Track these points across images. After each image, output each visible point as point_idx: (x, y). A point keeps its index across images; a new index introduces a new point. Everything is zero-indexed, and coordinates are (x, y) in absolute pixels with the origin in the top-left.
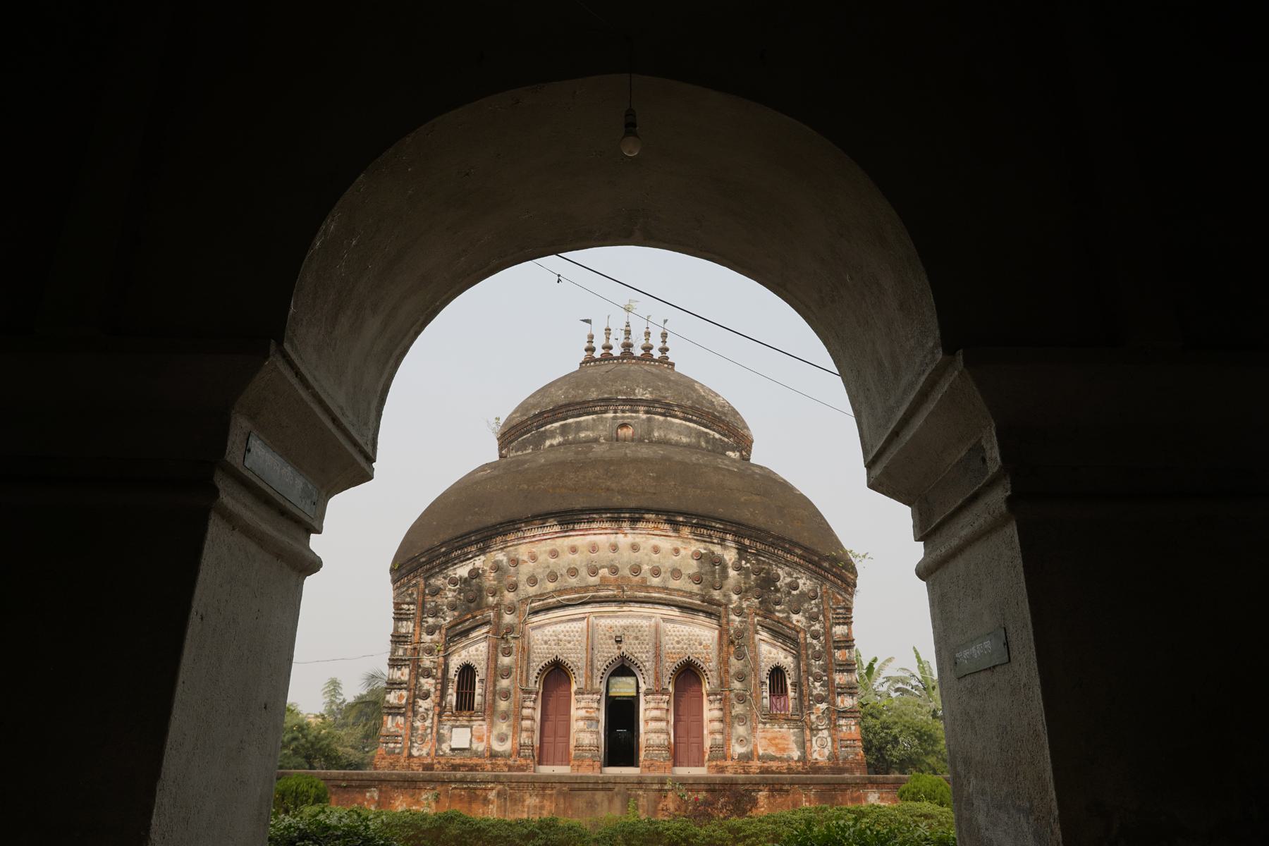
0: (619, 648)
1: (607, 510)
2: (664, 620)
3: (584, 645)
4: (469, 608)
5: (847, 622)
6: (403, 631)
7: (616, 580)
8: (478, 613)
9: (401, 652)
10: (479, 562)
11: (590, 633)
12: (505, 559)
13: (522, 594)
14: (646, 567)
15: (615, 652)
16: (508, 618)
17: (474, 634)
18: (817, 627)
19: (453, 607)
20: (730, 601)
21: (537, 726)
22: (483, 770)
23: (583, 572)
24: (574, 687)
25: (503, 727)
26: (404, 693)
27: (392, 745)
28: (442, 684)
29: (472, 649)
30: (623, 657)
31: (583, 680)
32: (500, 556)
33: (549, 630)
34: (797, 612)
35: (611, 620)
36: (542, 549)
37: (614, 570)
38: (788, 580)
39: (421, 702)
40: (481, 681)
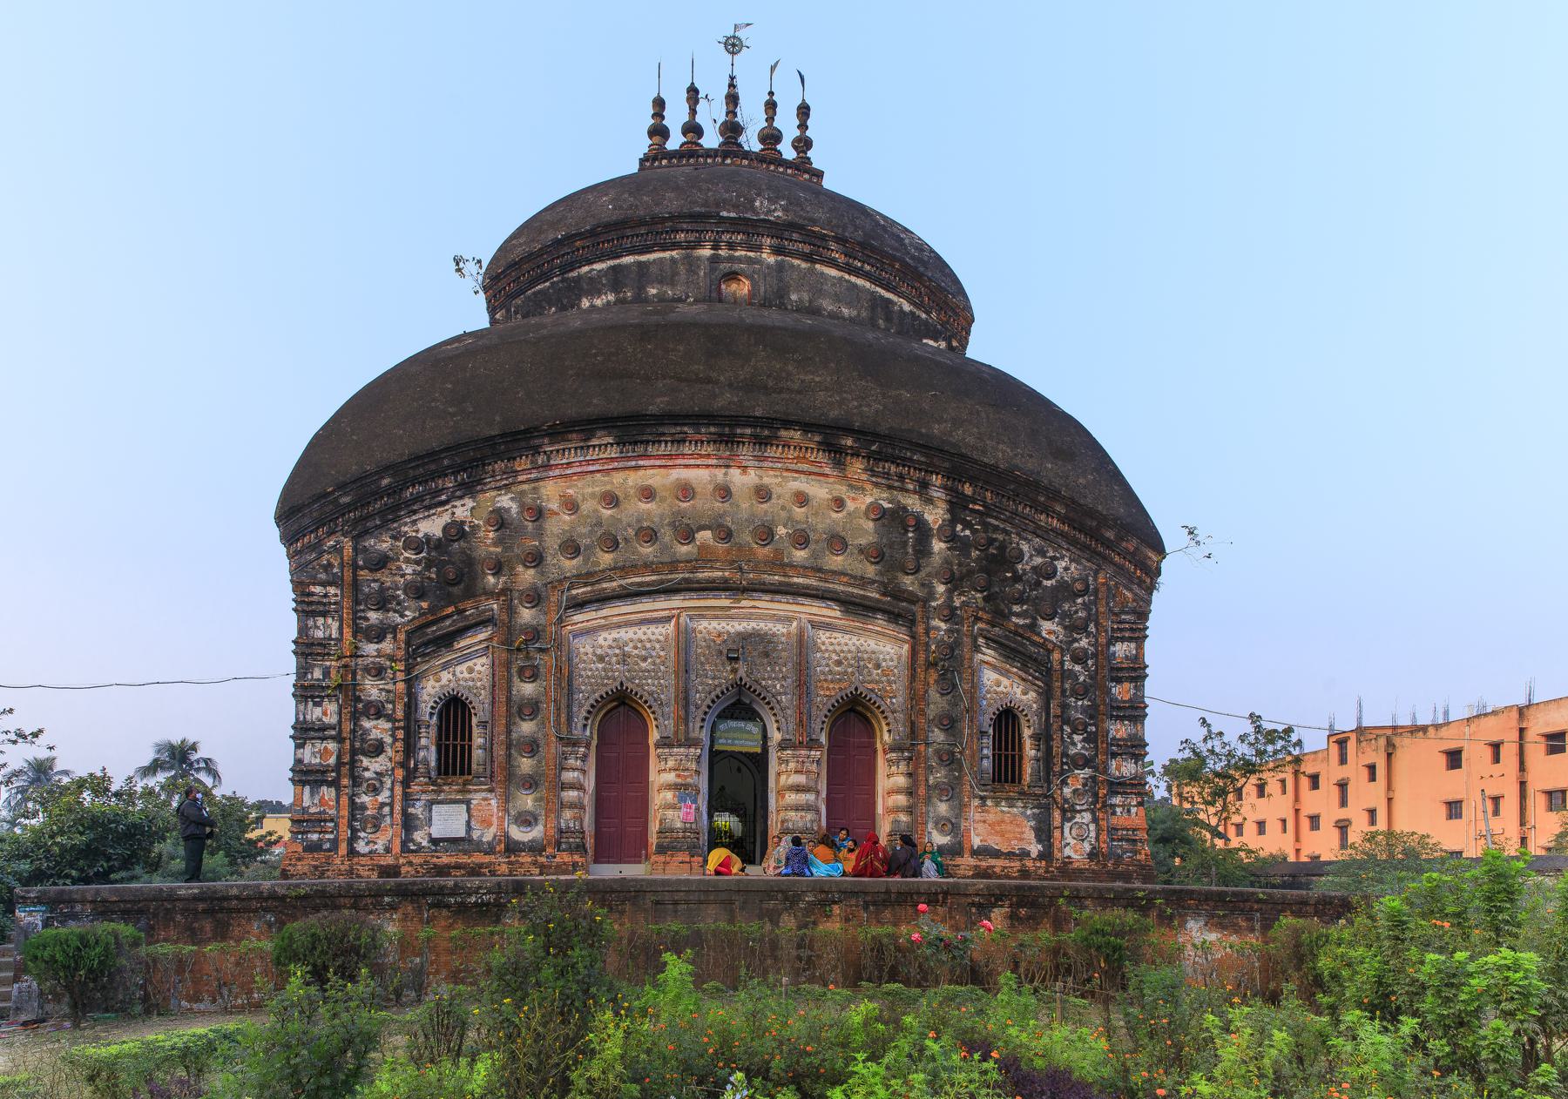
0: (734, 671)
1: (709, 418)
2: (815, 625)
3: (671, 664)
4: (449, 595)
5: (1139, 637)
6: (320, 634)
7: (728, 551)
8: (469, 604)
9: (318, 674)
10: (462, 510)
11: (684, 640)
12: (514, 507)
13: (553, 574)
14: (781, 531)
15: (725, 675)
16: (526, 615)
17: (462, 644)
18: (1084, 643)
19: (417, 591)
20: (931, 595)
21: (588, 800)
22: (493, 873)
23: (667, 535)
24: (654, 736)
25: (527, 801)
26: (332, 746)
27: (315, 837)
28: (407, 729)
29: (463, 667)
30: (739, 686)
31: (670, 723)
32: (505, 501)
33: (605, 638)
34: (1050, 618)
35: (720, 621)
36: (587, 489)
37: (726, 535)
38: (1038, 560)
39: (366, 762)
40: (483, 724)
